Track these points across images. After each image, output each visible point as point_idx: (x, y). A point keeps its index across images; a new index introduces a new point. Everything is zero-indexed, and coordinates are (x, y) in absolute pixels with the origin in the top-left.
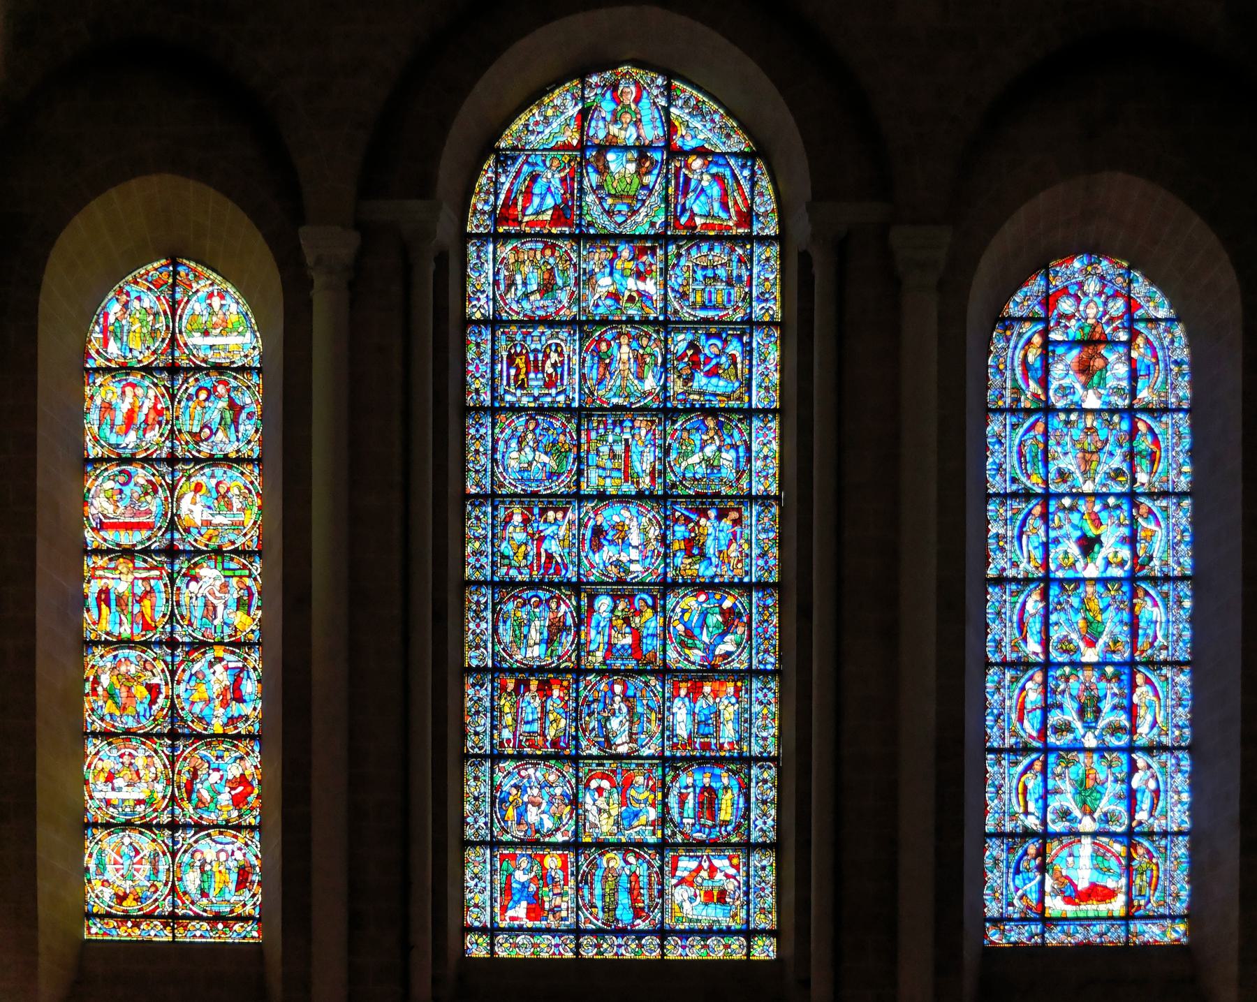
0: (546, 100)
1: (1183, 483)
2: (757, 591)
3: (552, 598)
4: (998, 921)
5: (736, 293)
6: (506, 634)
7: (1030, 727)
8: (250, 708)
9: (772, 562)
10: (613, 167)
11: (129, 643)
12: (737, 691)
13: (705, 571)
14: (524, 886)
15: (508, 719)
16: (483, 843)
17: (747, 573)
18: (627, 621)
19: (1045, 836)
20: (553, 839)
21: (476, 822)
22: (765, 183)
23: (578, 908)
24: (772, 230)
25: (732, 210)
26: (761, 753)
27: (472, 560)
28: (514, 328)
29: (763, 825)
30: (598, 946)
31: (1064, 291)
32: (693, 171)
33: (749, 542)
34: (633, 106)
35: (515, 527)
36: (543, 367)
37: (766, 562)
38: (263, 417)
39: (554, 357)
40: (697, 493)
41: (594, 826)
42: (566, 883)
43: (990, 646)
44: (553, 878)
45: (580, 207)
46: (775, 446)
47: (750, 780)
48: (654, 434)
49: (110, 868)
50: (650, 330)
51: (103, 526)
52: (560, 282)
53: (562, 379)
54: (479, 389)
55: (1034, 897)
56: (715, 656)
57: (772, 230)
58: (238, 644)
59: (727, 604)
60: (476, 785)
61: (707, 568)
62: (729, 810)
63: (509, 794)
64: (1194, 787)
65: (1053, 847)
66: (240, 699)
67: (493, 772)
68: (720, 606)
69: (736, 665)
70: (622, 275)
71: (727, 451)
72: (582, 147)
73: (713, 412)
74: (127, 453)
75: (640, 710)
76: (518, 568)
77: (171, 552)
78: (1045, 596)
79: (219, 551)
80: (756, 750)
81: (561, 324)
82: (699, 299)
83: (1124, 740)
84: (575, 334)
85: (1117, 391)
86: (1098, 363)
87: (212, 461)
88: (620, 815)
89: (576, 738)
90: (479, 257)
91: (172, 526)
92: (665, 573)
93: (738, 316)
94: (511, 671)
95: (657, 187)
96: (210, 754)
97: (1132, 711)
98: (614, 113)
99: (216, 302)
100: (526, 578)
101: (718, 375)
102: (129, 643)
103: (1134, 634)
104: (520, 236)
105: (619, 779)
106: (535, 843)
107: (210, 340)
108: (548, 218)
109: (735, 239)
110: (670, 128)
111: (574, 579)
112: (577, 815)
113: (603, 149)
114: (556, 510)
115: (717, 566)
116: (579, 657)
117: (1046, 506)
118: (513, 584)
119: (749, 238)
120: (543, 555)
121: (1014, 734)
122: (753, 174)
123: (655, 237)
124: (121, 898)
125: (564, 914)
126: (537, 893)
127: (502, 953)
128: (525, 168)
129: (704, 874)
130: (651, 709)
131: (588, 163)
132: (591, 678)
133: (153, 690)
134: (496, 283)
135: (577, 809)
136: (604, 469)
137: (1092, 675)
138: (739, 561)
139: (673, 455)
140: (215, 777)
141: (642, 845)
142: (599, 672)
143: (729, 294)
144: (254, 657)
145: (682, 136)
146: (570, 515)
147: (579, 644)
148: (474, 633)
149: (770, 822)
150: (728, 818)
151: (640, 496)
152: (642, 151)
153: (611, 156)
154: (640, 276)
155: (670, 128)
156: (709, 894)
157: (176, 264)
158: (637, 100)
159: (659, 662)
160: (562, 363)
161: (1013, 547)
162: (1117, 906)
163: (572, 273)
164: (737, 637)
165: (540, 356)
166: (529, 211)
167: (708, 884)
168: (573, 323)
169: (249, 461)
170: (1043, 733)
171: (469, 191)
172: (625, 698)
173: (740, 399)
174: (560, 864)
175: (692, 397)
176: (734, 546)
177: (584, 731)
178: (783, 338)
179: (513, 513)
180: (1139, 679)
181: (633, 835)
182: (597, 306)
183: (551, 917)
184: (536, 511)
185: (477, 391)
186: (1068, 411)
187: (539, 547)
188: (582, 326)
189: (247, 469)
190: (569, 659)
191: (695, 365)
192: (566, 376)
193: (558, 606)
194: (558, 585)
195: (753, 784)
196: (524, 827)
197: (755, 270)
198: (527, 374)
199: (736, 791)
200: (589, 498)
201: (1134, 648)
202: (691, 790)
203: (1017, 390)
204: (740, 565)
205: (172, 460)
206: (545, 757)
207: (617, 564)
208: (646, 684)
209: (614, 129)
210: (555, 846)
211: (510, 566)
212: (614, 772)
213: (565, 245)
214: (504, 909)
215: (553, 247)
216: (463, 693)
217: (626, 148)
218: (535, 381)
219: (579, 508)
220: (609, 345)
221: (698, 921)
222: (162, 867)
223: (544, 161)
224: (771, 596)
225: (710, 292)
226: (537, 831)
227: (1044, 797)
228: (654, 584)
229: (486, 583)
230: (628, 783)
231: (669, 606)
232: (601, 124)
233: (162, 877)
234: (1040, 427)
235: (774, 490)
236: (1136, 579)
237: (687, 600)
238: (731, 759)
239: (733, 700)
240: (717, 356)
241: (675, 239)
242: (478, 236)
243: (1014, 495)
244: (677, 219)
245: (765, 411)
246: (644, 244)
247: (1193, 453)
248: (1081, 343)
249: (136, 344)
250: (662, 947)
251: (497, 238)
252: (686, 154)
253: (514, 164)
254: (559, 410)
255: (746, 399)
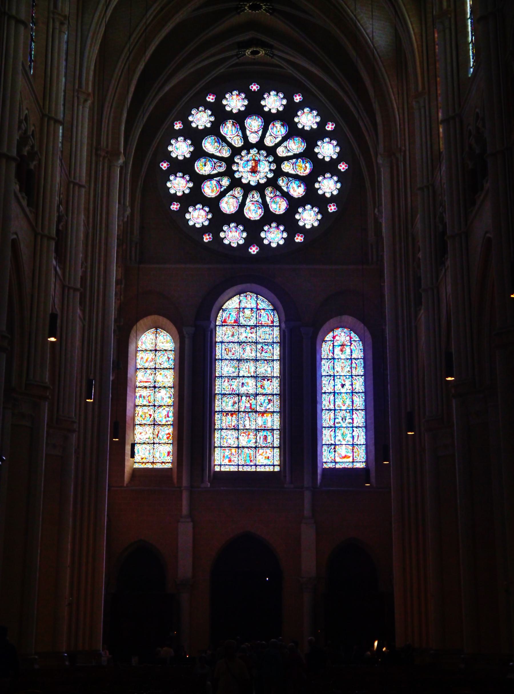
1: (362, 373)
4: (325, 463)
5: (271, 336)
7: (331, 423)
8: (171, 419)
11: (145, 406)
13: (264, 392)
15: (224, 421)
16: (219, 447)
18: (249, 401)
19: (335, 445)
22: (276, 315)
24: (278, 324)
29: (277, 443)
31: (337, 335)
38: (174, 360)
39: (234, 349)
43: (323, 406)
46: (279, 367)
49: (140, 452)
51: (140, 382)
52: (235, 334)
54: (218, 356)
55: (333, 458)
58: (168, 406)
59: (269, 398)
60: (217, 435)
64: (366, 435)
65: (337, 447)
66: (168, 417)
72: (240, 308)
74: (146, 367)
77: (155, 387)
78: (334, 396)
79: (165, 387)
81: (235, 343)
83: (351, 425)
85: (348, 355)
86: (344, 349)
87: (164, 369)
91: (155, 382)
94: (225, 412)
96: (162, 428)
97: (353, 419)
99: (165, 337)
102: (145, 406)
103: (353, 404)
104: (227, 325)
105: (247, 434)
107: (163, 345)
109: (270, 326)
110: (257, 304)
113: (244, 309)
117: (334, 378)
118: (225, 394)
119: (273, 326)
121: (328, 424)
124: (142, 459)
133: (150, 415)
137: (344, 412)
139: (258, 368)
140: (163, 433)
141: (251, 447)
142: (243, 412)
144: (172, 408)
151: (251, 376)
152: (252, 309)
153: (245, 310)
154: (251, 333)
155: (257, 304)
156: (266, 457)
157: (157, 329)
161: (326, 385)
162: (351, 460)
163: (237, 333)
167: (265, 455)
168: (238, 342)
169: (171, 369)
170: (334, 424)
171: (217, 316)
172: (248, 417)
178: (280, 345)
180: (354, 413)
186: (338, 359)
188: (240, 343)
189: (171, 370)
191: (262, 350)
194: (235, 394)
197: (275, 332)
200: (241, 377)
201: (353, 407)
203: (328, 355)
205: (155, 369)
206: (232, 429)
207: (247, 390)
209: (246, 305)
210: (234, 447)
213: (236, 327)
222: (151, 451)
227: (335, 437)
230: (249, 435)
233: (151, 454)
234: (333, 362)
235: (279, 375)
236: (353, 393)
238: (270, 430)
241: (258, 326)
243: (327, 376)
245: (277, 360)
247: (364, 367)
248: (341, 345)
249: (148, 345)
252: (260, 309)
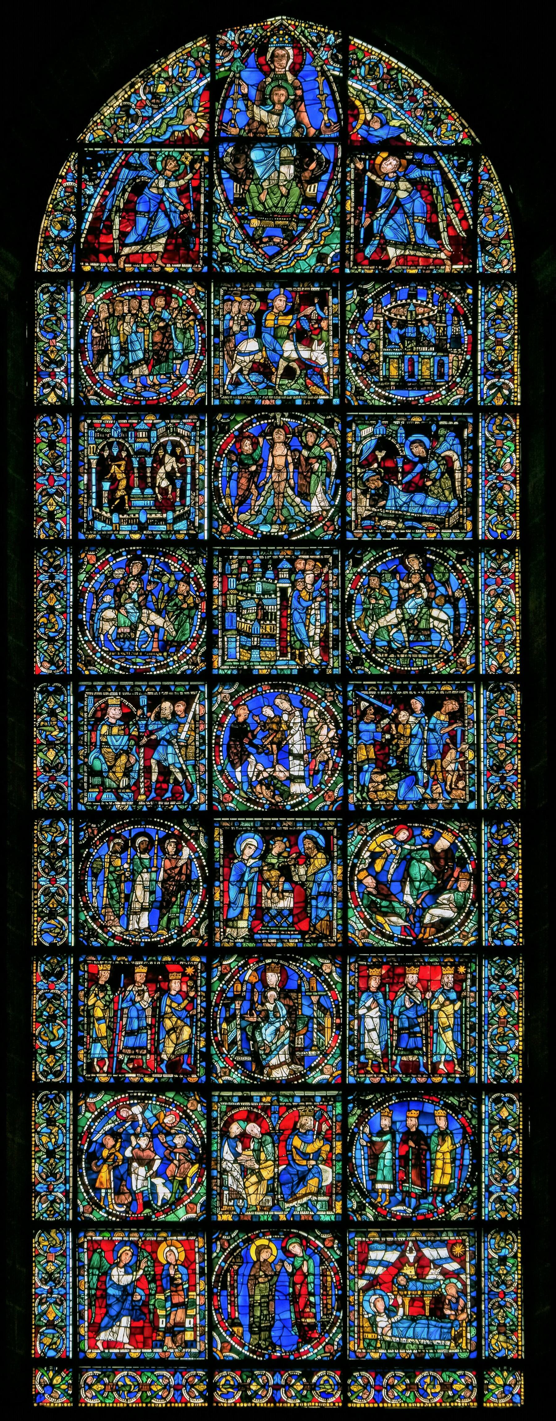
0: (156, 69)
2: (490, 825)
3: (168, 836)
5: (453, 361)
6: (97, 894)
9: (512, 779)
10: (259, 170)
12: (459, 981)
14: (126, 1291)
16: (60, 1225)
17: (472, 795)
18: (286, 872)
20: (171, 1218)
21: (50, 1192)
22: (495, 194)
23: (212, 1327)
24: (507, 265)
25: (444, 235)
26: (497, 1078)
27: (42, 778)
28: (108, 419)
29: (503, 1190)
30: (243, 1387)
32: (385, 177)
33: (475, 747)
34: (290, 77)
35: (111, 726)
36: (154, 478)
37: (503, 779)
39: (170, 463)
40: (394, 671)
41: (236, 1195)
42: (193, 1287)
44: (173, 1279)
45: (210, 233)
46: (514, 598)
47: (480, 1121)
48: (326, 581)
50: (319, 419)
53: (183, 496)
54: (53, 512)
56: (424, 926)
57: (507, 265)
59: (443, 844)
60: (49, 1131)
61: (410, 789)
62: (448, 1169)
63: (103, 1146)
67: (77, 1111)
68: (431, 848)
69: (456, 940)
70: (275, 337)
71: (440, 608)
72: (212, 141)
73: (418, 548)
75: (307, 1011)
76: (116, 791)
80: (489, 1073)
81: (182, 411)
82: (394, 372)
84: (202, 428)
88: (276, 1177)
89: (207, 1057)
90: (53, 310)
92: (346, 797)
93: (456, 398)
94: (105, 952)
95: (328, 200)
98: (261, 88)
100: (126, 805)
101: (424, 490)
104: (117, 277)
106: (145, 1224)
108: (160, 249)
109: (449, 280)
111: (203, 807)
112: (210, 1178)
114: (174, 700)
115: (425, 786)
116: (211, 930)
118: (107, 815)
119: (471, 278)
120: (155, 768)
122: (475, 175)
123: (326, 278)
125: (189, 1336)
126: (146, 1304)
127: (90, 1399)
128: (125, 172)
129: (409, 1271)
130: (324, 1010)
131: (222, 165)
132: (231, 961)
134: (79, 349)
135: (209, 1169)
136: (249, 635)
138: (460, 778)
139: (357, 613)
141: (312, 1225)
143: (441, 364)
145: (366, 123)
146: (195, 707)
147: (211, 908)
148: (46, 893)
149: (511, 1185)
150: (446, 1181)
151: (305, 676)
152: (304, 147)
153: (256, 155)
154: (302, 337)
155: (348, 110)
158: (295, 70)
159: (336, 936)
160: (183, 472)
164: (458, 897)
165: (149, 461)
166: (131, 238)
168: (200, 408)
172: (284, 993)
173: (459, 526)
174: (182, 1257)
175: (384, 523)
176: (452, 754)
177: (220, 1045)
178: (525, 432)
179: (107, 705)
181: (297, 1208)
182: (237, 384)
183: (168, 1341)
184: (143, 701)
185: (51, 515)
187: (147, 759)
190: (197, 935)
191: (389, 474)
192: (188, 493)
193: (178, 851)
194: (177, 817)
195: (484, 1129)
196: (126, 1199)
198: (129, 488)
199: (458, 1139)
200: (226, 680)
202: (388, 1137)
204: (461, 785)
206: (159, 1088)
207: (270, 782)
208: (317, 970)
209: (261, 114)
210: (176, 1228)
211: (103, 788)
212: (266, 1109)
214: (95, 1329)
215: (168, 294)
216: (28, 988)
217: (280, 142)
218: (141, 501)
219: (211, 696)
220: (255, 444)
221: (401, 1345)
223: (153, 163)
224: (511, 831)
225: (412, 362)
226: (147, 1205)
228: (328, 814)
229: (64, 814)
231: (351, 849)
232: (241, 105)
235: (513, 665)
237: (380, 838)
238: (450, 1089)
239: (453, 995)
240: (423, 460)
242: (51, 277)
244: (359, 249)
245: (499, 545)
246: (309, 289)
250: (344, 1388)
251: (81, 280)
253: (107, 166)
254: (178, 544)
255: (469, 526)
